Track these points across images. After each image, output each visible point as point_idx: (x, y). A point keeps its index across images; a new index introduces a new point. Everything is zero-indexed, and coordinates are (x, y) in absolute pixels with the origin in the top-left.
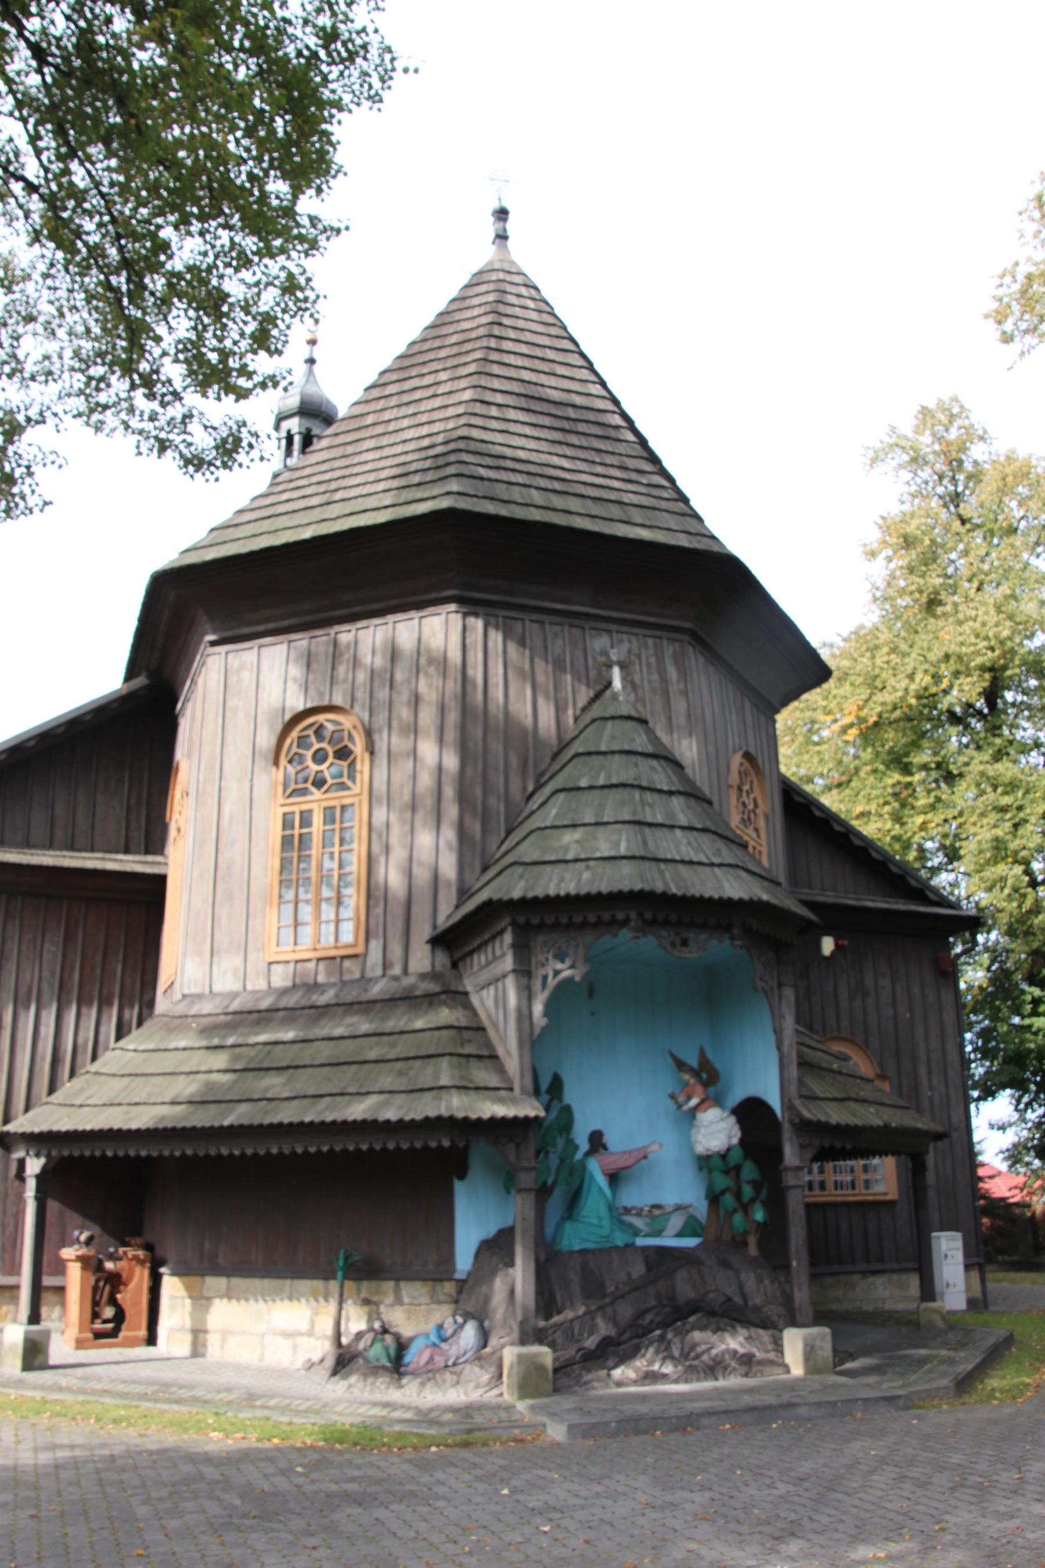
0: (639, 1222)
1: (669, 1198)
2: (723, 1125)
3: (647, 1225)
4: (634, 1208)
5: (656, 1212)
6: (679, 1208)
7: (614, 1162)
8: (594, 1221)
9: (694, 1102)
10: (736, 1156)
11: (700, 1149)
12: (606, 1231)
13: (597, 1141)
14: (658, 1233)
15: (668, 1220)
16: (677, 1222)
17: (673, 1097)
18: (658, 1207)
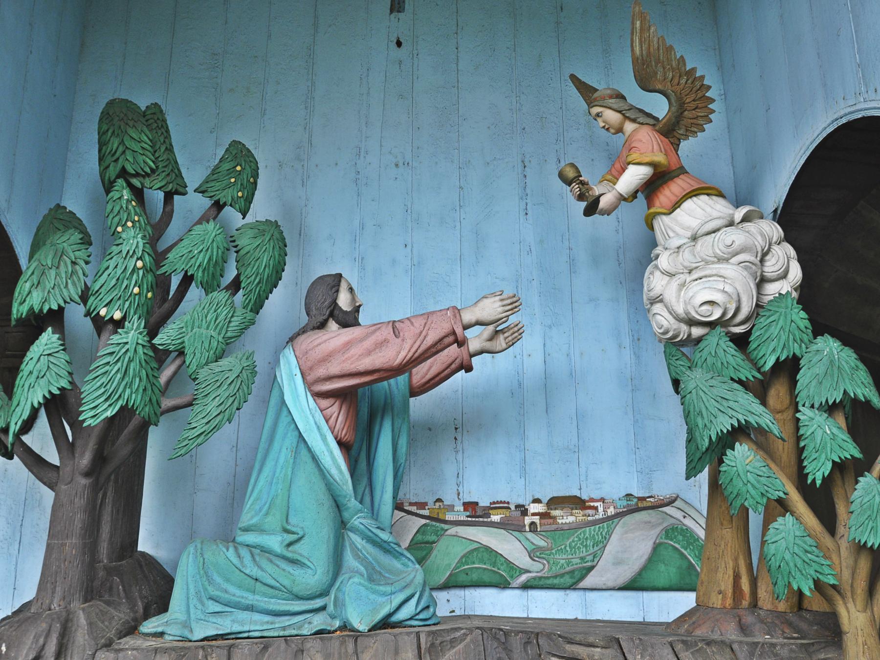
0: (510, 548)
1: (610, 480)
2: (735, 237)
3: (534, 553)
4: (499, 506)
5: (565, 517)
6: (636, 505)
7: (344, 351)
8: (275, 542)
9: (634, 176)
10: (784, 333)
11: (663, 320)
12: (311, 578)
13: (328, 307)
14: (573, 580)
15: (602, 543)
16: (630, 546)
17: (571, 178)
18: (577, 503)
